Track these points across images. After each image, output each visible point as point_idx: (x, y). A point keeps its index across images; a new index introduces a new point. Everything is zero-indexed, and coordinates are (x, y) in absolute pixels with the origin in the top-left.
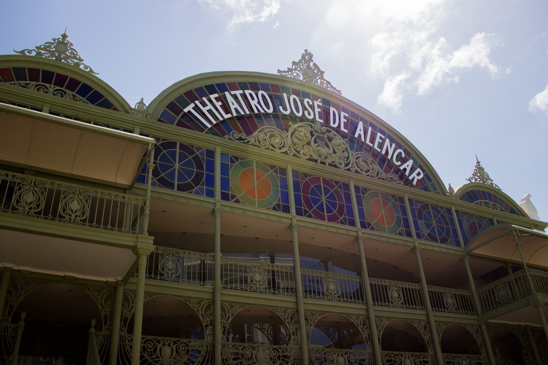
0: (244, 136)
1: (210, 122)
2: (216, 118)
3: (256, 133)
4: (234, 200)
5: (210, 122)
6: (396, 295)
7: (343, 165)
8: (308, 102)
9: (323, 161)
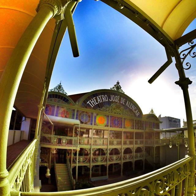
0: (100, 109)
1: (93, 106)
2: (94, 104)
3: (103, 108)
5: (93, 106)
6: (128, 142)
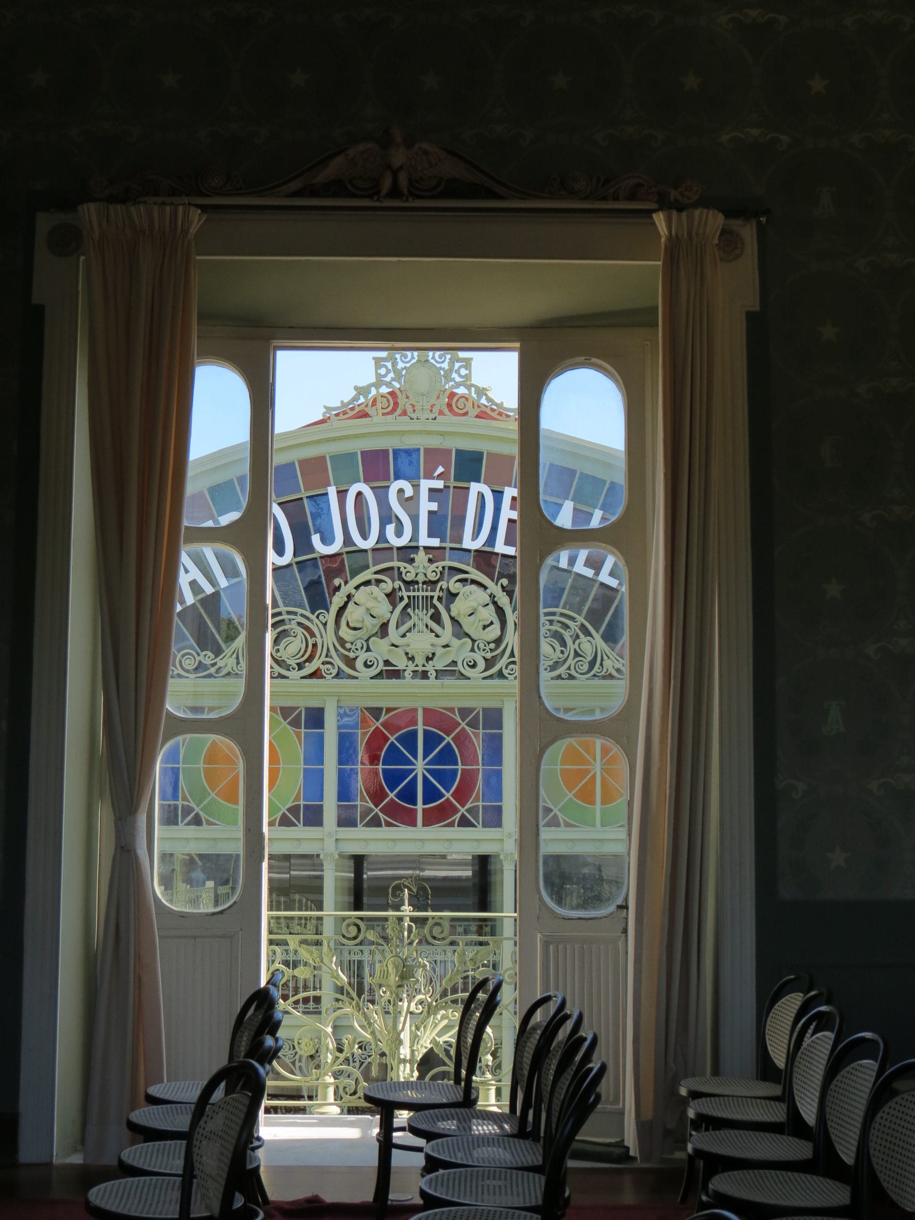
0: (207, 657)
4: (189, 818)
7: (481, 665)
8: (401, 491)
9: (420, 669)
